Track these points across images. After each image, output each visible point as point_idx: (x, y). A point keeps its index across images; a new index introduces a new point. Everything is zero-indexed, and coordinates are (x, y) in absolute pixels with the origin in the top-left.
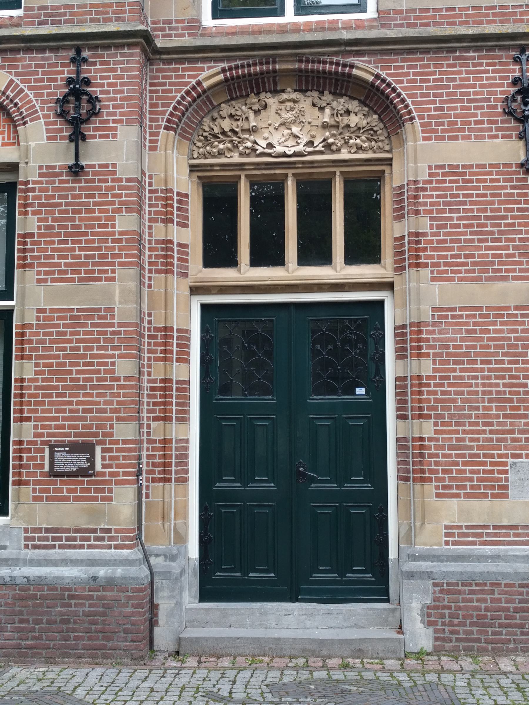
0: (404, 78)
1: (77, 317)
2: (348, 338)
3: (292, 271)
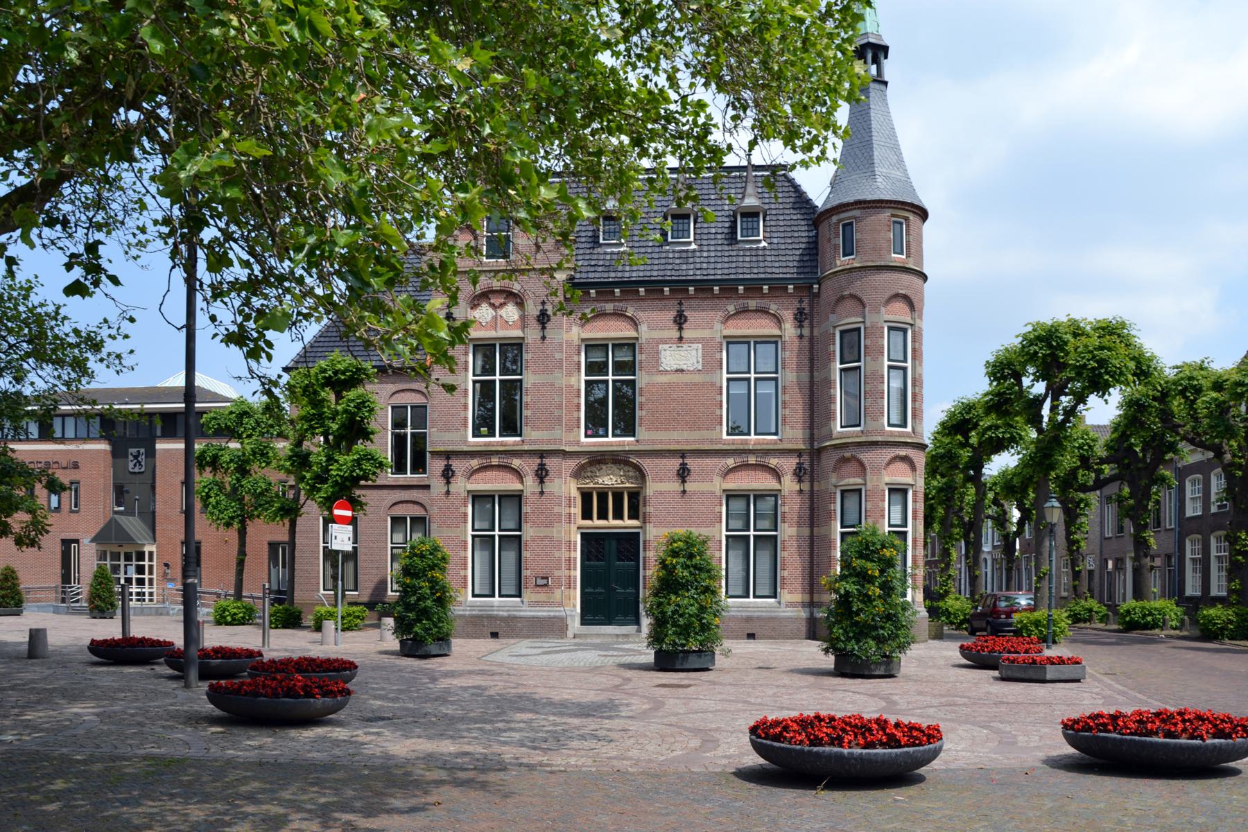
0: (646, 464)
1: (542, 539)
3: (612, 522)
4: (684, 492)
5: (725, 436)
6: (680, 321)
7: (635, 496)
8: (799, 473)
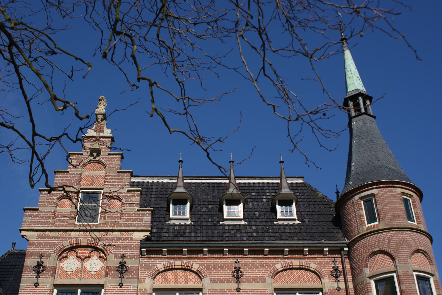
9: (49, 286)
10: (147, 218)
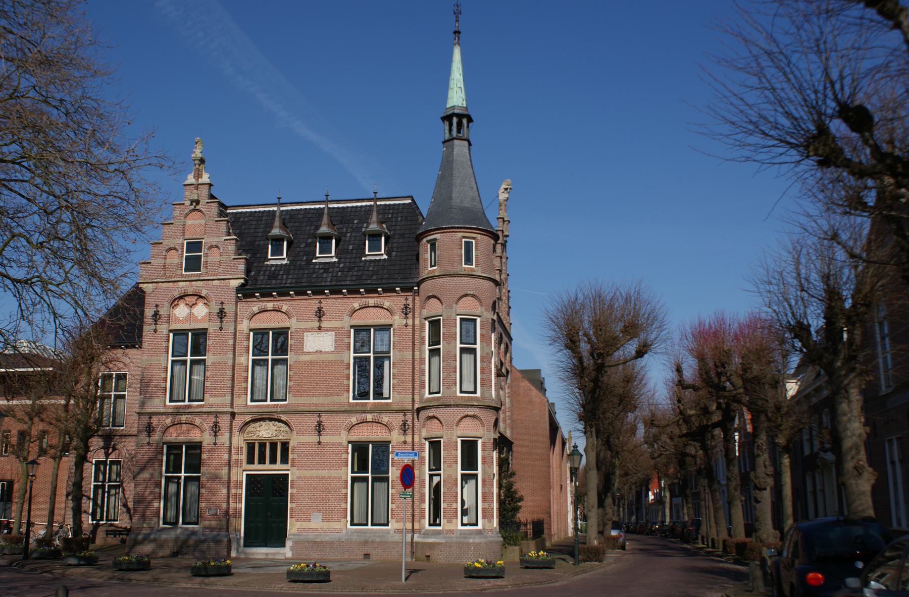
2: (279, 484)
3: (268, 466)
4: (319, 443)
5: (351, 401)
6: (320, 314)
7: (285, 446)
8: (404, 428)
9: (165, 332)
10: (242, 266)
